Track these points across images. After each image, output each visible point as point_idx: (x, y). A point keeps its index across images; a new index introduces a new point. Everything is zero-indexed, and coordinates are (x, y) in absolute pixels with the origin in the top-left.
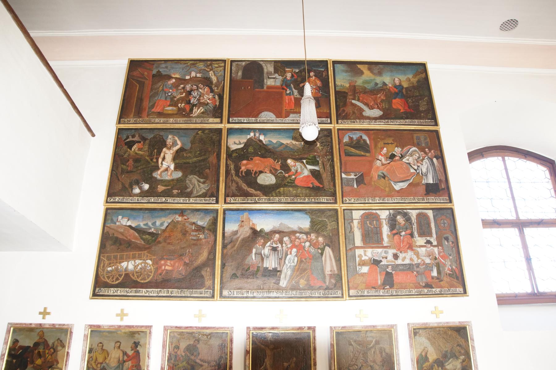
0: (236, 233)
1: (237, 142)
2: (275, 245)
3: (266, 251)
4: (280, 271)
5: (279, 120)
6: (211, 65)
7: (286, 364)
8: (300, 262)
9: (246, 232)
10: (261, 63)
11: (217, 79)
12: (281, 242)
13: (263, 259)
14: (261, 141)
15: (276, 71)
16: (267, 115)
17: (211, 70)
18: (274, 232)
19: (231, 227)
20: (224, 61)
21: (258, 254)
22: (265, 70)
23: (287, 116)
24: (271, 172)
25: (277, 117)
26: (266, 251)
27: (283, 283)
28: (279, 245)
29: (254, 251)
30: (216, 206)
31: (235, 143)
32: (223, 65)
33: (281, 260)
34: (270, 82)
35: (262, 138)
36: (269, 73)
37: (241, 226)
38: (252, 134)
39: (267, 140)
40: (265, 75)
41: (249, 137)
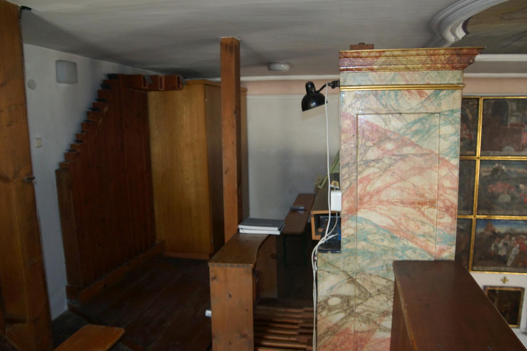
0: (482, 234)
1: (486, 169)
2: (506, 242)
3: (501, 245)
4: (508, 257)
5: (517, 153)
6: (467, 103)
7: (505, 306)
8: (521, 253)
9: (489, 233)
10: (507, 101)
11: (473, 116)
12: (510, 239)
13: (498, 250)
14: (503, 170)
15: (518, 109)
16: (509, 148)
17: (468, 108)
18: (505, 234)
19: (481, 230)
20: (478, 99)
21: (496, 246)
22: (510, 108)
23: (522, 150)
24: (508, 193)
25: (516, 151)
26: (501, 245)
27: (509, 263)
28: (509, 242)
29: (493, 245)
30: (472, 217)
31: (485, 171)
32: (476, 102)
33: (509, 251)
34: (513, 120)
35: (504, 167)
36: (513, 111)
37: (486, 230)
38: (497, 165)
39: (507, 169)
40: (509, 112)
41: (494, 167)
